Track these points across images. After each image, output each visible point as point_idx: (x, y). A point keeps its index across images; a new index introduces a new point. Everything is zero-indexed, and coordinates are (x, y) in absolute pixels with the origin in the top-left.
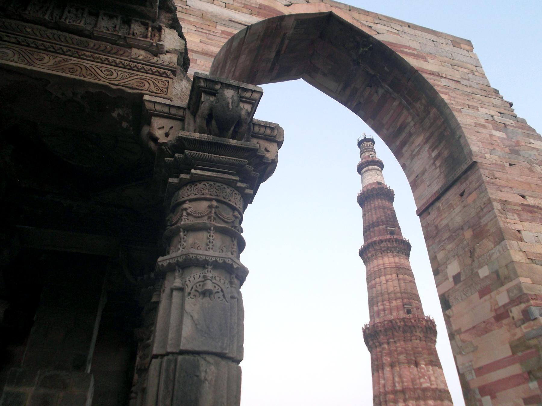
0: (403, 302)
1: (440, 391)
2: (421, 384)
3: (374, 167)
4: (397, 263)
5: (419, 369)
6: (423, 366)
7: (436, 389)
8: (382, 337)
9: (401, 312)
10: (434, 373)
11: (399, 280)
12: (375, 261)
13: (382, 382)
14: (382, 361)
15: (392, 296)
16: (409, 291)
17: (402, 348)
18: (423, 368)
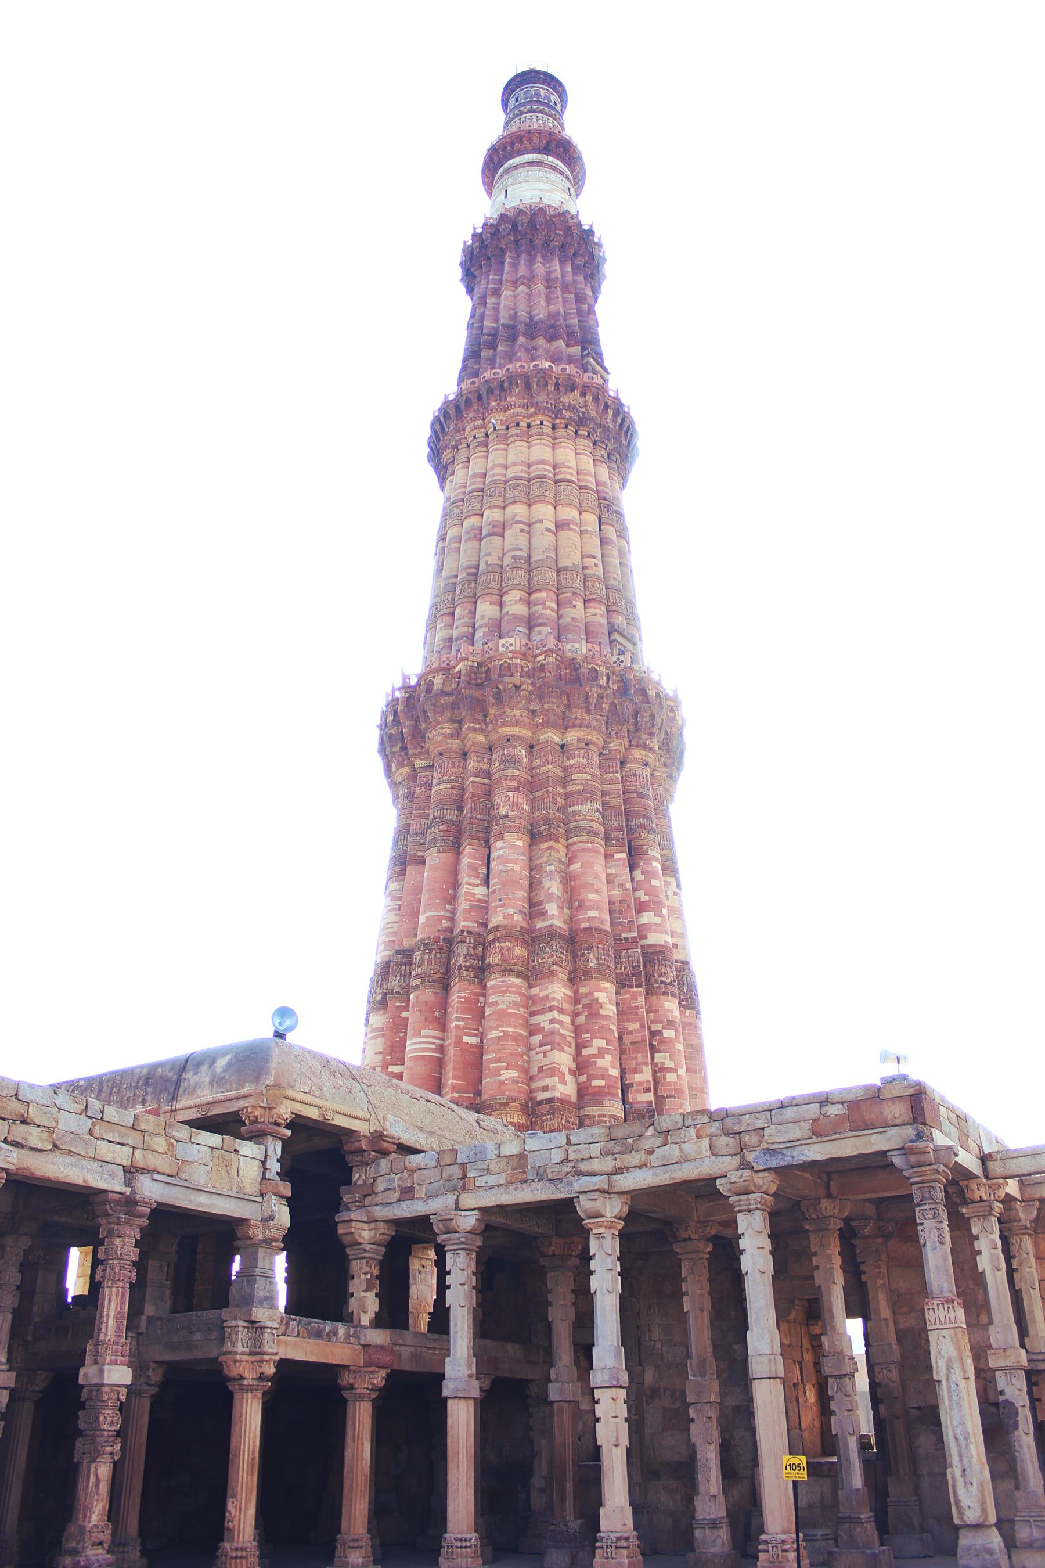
4: (604, 484)
11: (603, 541)
13: (472, 889)
18: (654, 875)
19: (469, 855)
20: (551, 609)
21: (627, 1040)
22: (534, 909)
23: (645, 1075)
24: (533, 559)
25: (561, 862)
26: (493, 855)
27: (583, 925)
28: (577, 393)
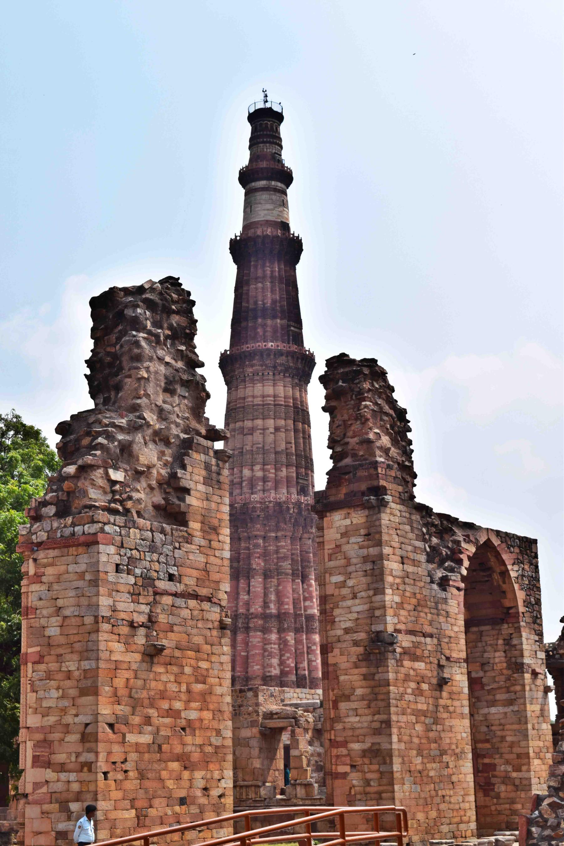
0: (297, 474)
2: (306, 609)
5: (305, 587)
6: (313, 582)
9: (294, 490)
11: (296, 431)
12: (259, 386)
13: (244, 597)
14: (250, 564)
17: (288, 550)
19: (242, 584)
20: (272, 473)
21: (298, 652)
22: (266, 605)
23: (305, 664)
24: (266, 448)
26: (251, 584)
27: (283, 611)
28: (284, 357)
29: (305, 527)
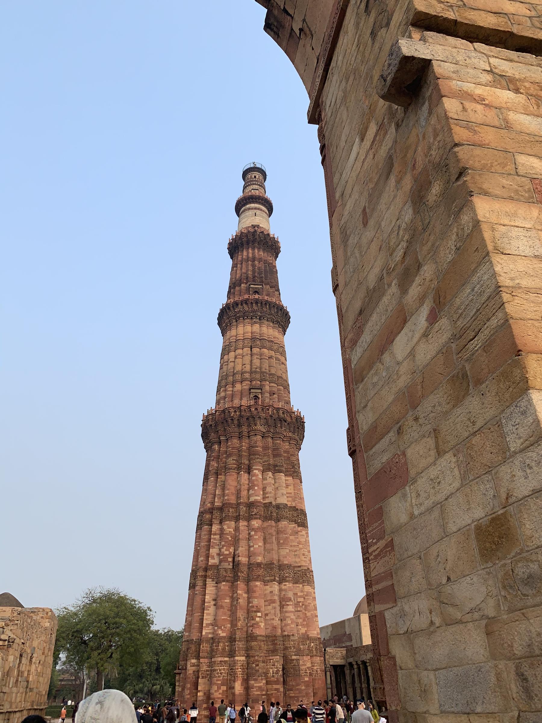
0: (251, 385)
1: (278, 507)
3: (253, 205)
4: (254, 332)
7: (271, 503)
8: (213, 434)
10: (275, 483)
15: (238, 377)
16: (263, 370)
18: (255, 475)
20: (230, 391)
25: (222, 481)
28: (240, 306)
29: (249, 426)
